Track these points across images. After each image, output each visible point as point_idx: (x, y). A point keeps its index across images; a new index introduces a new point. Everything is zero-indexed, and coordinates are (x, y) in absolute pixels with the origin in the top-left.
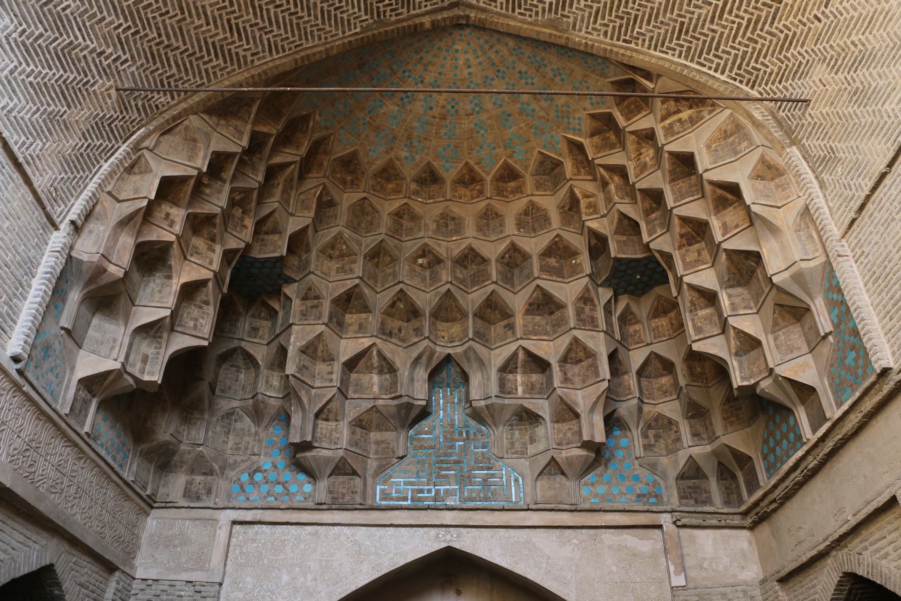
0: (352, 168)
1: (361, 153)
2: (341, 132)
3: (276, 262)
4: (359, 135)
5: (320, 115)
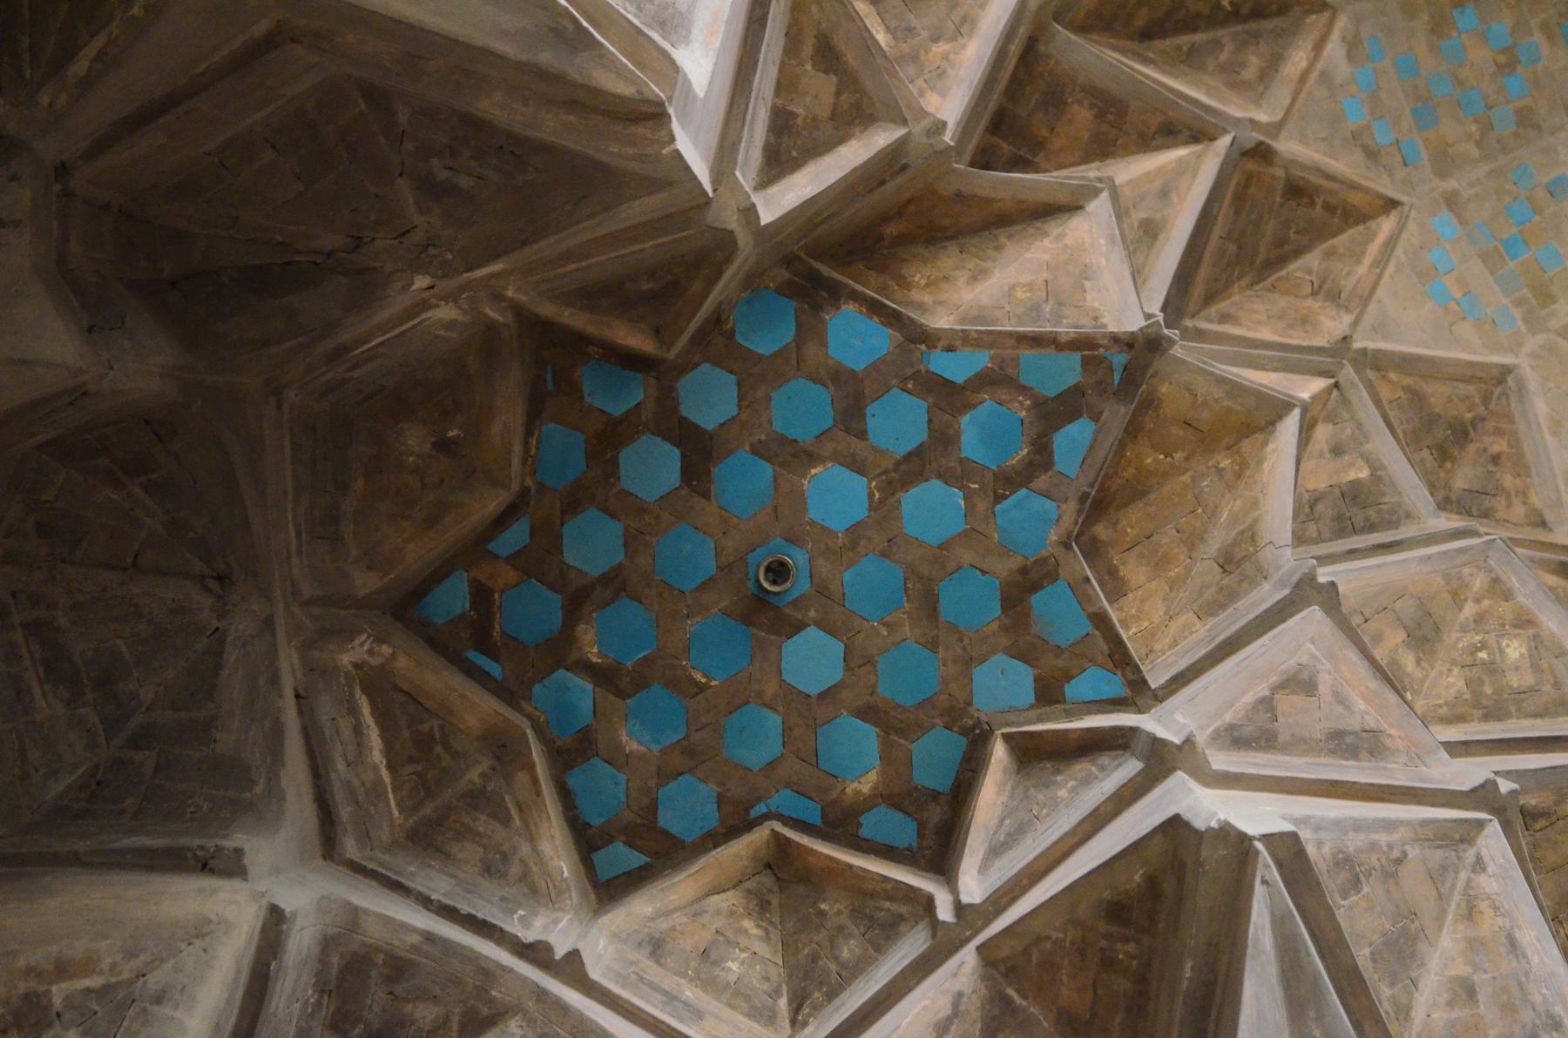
0: (1464, 477)
1: (1540, 406)
2: (1445, 224)
3: (1055, 412)
4: (1546, 296)
5: (1353, 47)
